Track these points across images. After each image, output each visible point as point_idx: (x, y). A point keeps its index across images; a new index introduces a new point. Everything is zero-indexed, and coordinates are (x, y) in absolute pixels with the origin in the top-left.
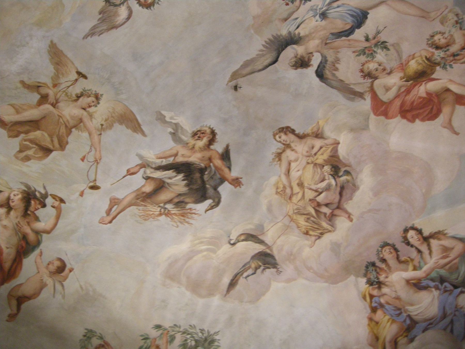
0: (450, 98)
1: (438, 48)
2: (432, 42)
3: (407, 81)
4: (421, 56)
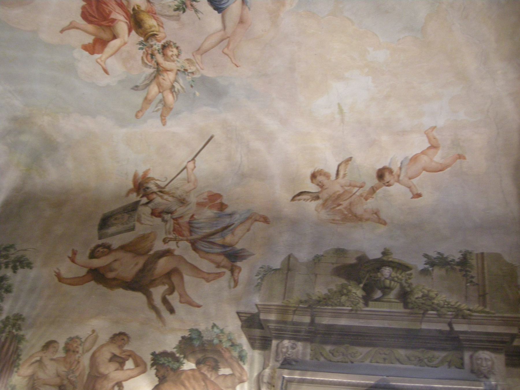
0: (105, 35)
1: (164, 47)
2: (171, 46)
3: (134, 9)
4: (159, 31)
